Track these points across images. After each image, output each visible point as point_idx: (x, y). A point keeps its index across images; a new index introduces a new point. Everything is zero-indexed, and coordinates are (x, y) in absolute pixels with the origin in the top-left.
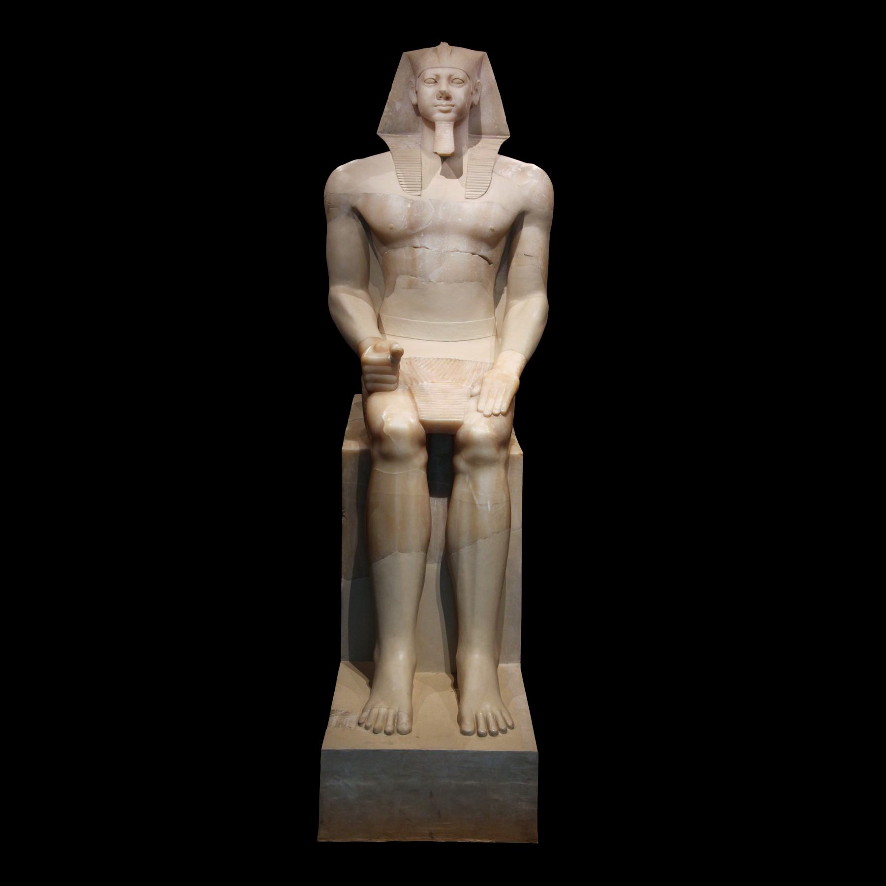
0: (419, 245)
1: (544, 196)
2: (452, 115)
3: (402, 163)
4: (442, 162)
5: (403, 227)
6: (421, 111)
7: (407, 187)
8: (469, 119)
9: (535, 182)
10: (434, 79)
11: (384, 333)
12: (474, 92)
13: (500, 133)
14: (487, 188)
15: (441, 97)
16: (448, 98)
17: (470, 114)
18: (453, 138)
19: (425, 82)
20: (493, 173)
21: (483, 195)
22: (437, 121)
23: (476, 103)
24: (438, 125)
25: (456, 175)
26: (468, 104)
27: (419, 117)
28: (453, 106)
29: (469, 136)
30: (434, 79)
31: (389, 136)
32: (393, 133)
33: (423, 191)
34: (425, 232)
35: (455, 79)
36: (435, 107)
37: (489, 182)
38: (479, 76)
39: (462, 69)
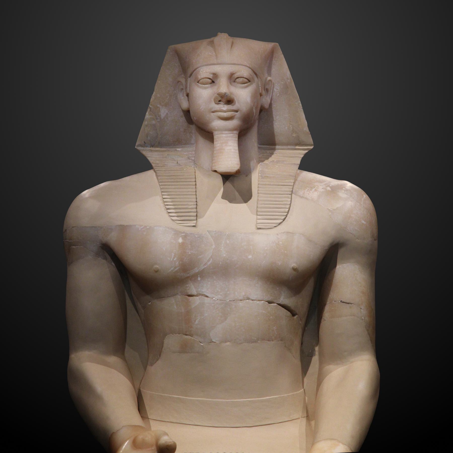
0: (194, 292)
1: (363, 222)
2: (235, 123)
3: (169, 185)
4: (224, 183)
5: (172, 269)
6: (194, 118)
7: (178, 216)
8: (258, 126)
9: (350, 204)
10: (210, 79)
11: (148, 418)
12: (264, 92)
13: (299, 143)
14: (285, 214)
15: (220, 101)
16: (230, 102)
17: (260, 119)
18: (237, 151)
19: (198, 82)
20: (293, 195)
21: (280, 224)
22: (216, 130)
23: (267, 106)
24: (217, 136)
25: (243, 199)
26: (256, 108)
27: (191, 126)
28: (237, 111)
29: (259, 148)
30: (210, 79)
31: (151, 151)
32: (157, 147)
33: (200, 221)
34: (203, 274)
35: (238, 78)
36: (212, 114)
37: (288, 206)
38: (269, 72)
39: (248, 65)
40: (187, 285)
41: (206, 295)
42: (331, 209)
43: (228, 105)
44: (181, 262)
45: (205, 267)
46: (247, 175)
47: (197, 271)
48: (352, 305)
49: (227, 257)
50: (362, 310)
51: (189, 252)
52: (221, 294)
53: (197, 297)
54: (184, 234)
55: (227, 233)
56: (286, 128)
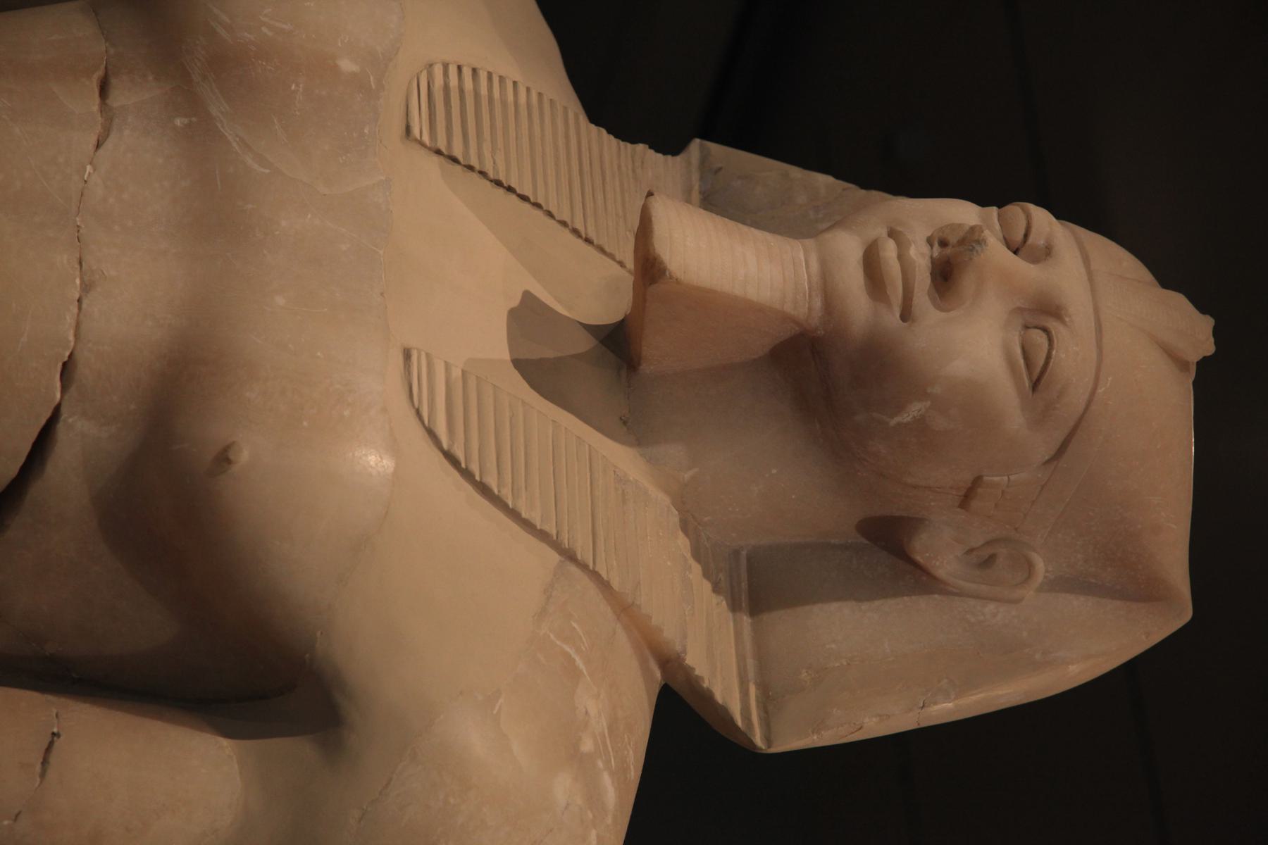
0: (121, 97)
4: (592, 329)
7: (446, 87)
10: (1026, 236)
13: (769, 701)
21: (431, 434)
28: (906, 315)
29: (736, 553)
30: (1026, 236)
39: (1100, 391)
40: (151, 78)
41: (104, 142)
42: (497, 708)
43: (931, 274)
44: (254, 48)
45: (235, 144)
46: (625, 423)
47: (214, 111)
48: (38, 779)
49: (277, 233)
50: (6, 823)
51: (297, 85)
52: (111, 200)
53: (95, 108)
54: (374, 87)
55: (381, 252)
56: (833, 646)
